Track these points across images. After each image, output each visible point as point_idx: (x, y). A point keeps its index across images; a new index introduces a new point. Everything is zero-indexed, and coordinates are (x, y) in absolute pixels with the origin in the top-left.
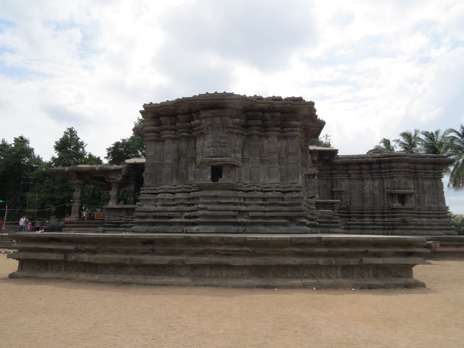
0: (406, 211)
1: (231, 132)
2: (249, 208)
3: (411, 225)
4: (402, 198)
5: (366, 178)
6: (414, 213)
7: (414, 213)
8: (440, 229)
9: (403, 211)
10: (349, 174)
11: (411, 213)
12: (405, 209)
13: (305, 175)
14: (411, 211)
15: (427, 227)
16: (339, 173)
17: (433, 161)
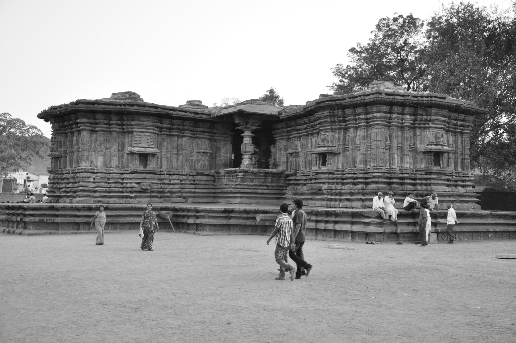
0: (324, 176)
1: (57, 133)
2: (62, 186)
3: (323, 194)
4: (323, 157)
5: (310, 134)
6: (337, 179)
7: (337, 179)
8: (362, 200)
9: (320, 176)
10: (299, 130)
11: (333, 179)
12: (323, 173)
13: (128, 154)
14: (330, 176)
15: (344, 197)
16: (294, 130)
17: (348, 103)
